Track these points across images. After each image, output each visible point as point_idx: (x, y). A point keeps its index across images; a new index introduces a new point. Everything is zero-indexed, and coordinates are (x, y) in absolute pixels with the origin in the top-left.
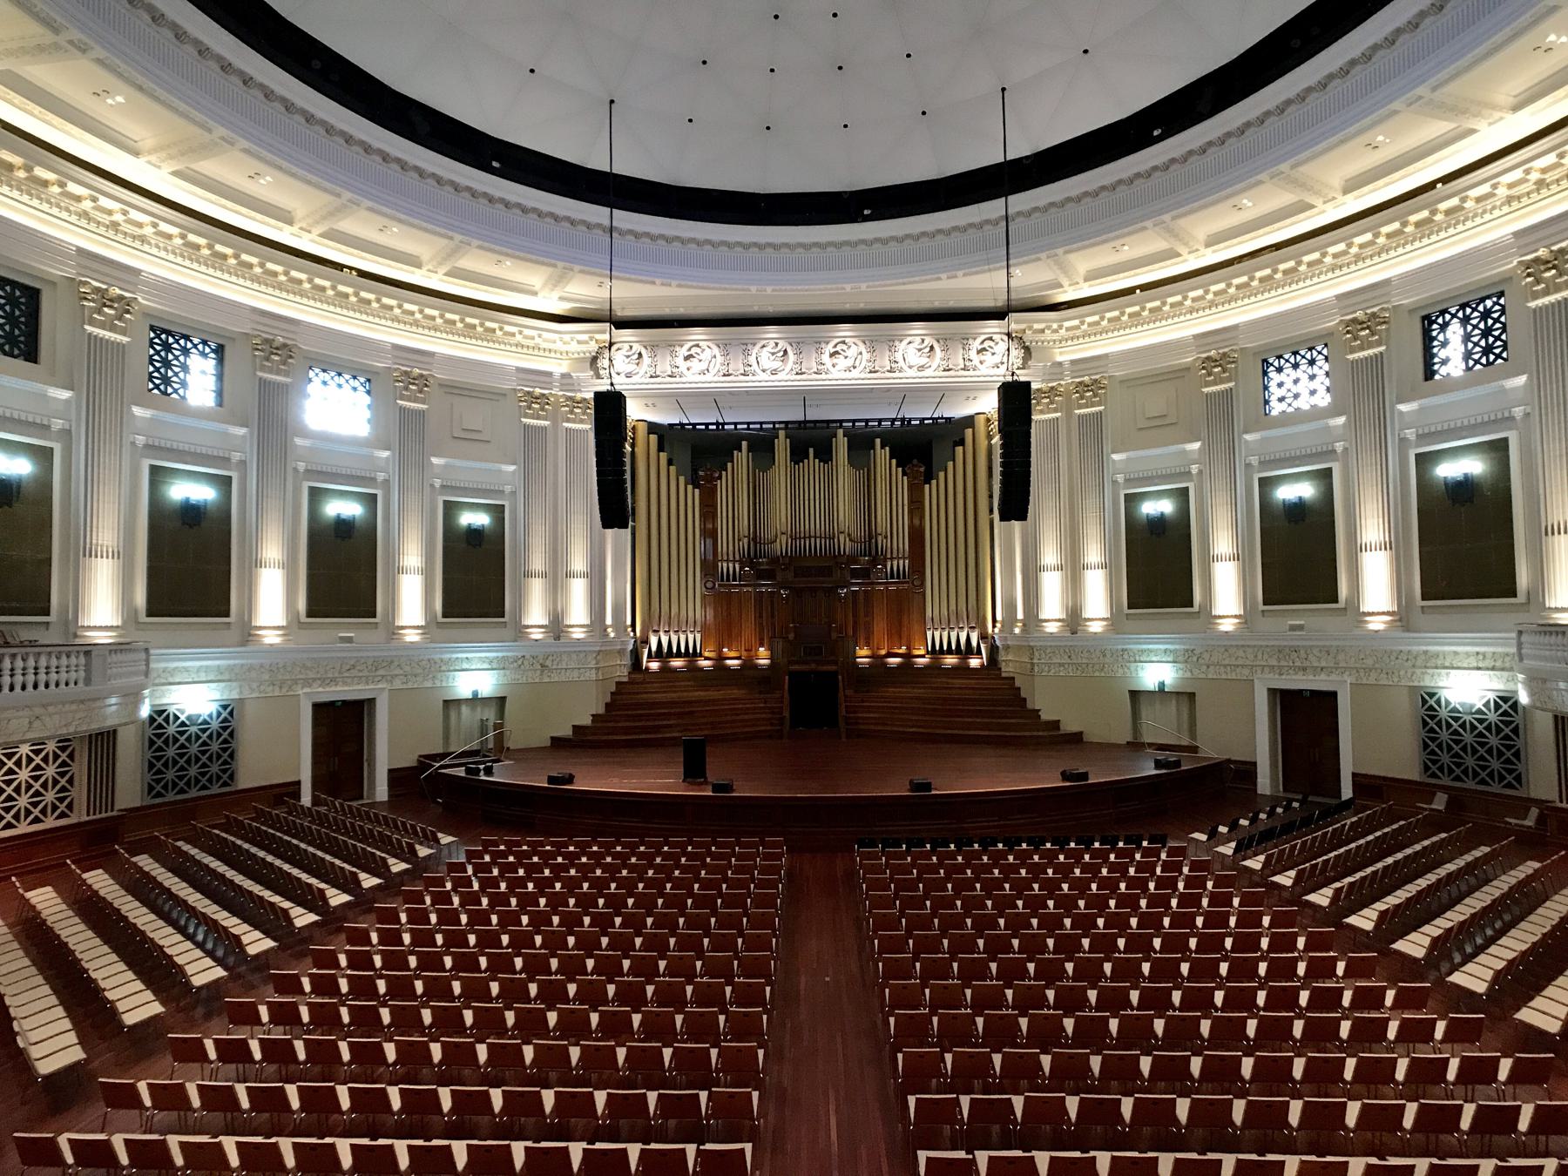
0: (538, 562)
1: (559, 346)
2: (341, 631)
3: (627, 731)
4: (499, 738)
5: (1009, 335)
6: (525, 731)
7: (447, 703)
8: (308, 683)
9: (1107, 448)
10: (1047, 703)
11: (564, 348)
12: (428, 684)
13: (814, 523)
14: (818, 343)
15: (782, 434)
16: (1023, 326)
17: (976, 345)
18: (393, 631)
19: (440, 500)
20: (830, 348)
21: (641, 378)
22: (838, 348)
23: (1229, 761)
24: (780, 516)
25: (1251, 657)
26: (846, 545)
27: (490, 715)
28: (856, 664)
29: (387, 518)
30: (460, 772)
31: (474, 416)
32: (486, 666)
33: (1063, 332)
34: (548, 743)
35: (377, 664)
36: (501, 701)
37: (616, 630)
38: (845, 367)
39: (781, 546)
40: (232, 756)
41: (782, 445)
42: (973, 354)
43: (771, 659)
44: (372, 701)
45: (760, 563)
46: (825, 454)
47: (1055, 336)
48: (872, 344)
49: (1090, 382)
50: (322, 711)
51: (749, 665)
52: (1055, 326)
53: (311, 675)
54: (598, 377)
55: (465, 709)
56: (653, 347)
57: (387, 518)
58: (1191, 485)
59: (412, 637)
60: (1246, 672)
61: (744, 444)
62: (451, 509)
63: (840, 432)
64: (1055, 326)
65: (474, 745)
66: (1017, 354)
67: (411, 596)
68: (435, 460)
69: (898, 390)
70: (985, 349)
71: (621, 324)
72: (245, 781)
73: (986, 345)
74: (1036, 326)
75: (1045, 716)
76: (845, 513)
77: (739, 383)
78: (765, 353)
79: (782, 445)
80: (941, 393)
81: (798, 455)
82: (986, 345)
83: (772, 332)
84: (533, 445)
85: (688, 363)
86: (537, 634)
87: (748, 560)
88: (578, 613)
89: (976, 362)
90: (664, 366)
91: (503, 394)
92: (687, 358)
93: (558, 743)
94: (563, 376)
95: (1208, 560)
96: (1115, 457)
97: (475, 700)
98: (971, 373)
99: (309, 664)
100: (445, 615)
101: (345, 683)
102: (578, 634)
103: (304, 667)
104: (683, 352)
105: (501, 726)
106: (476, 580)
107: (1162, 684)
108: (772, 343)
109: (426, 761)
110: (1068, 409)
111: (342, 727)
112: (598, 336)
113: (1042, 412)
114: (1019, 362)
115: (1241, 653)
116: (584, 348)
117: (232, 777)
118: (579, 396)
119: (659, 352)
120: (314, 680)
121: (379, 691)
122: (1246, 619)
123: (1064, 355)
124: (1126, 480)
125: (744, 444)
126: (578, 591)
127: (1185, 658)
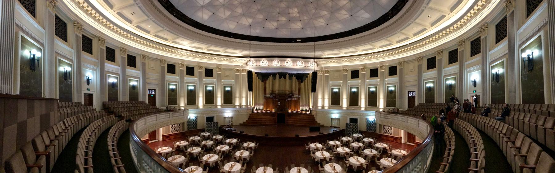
0: (238, 95)
1: (241, 61)
2: (210, 106)
6: (236, 123)
13: (282, 88)
14: (284, 61)
18: (216, 106)
26: (287, 92)
27: (230, 119)
30: (227, 129)
31: (227, 73)
38: (289, 64)
39: (277, 92)
41: (277, 75)
46: (285, 78)
48: (293, 61)
49: (327, 70)
51: (271, 112)
56: (256, 61)
59: (219, 107)
66: (316, 65)
67: (219, 101)
71: (251, 57)
72: (198, 128)
75: (318, 122)
76: (288, 88)
77: (271, 67)
79: (277, 75)
80: (304, 70)
81: (280, 78)
83: (276, 59)
84: (237, 77)
86: (237, 107)
87: (271, 94)
88: (244, 103)
90: (258, 64)
91: (232, 69)
93: (241, 124)
95: (342, 99)
97: (228, 117)
102: (244, 107)
104: (261, 62)
106: (228, 99)
110: (324, 74)
123: (323, 66)
126: (244, 100)
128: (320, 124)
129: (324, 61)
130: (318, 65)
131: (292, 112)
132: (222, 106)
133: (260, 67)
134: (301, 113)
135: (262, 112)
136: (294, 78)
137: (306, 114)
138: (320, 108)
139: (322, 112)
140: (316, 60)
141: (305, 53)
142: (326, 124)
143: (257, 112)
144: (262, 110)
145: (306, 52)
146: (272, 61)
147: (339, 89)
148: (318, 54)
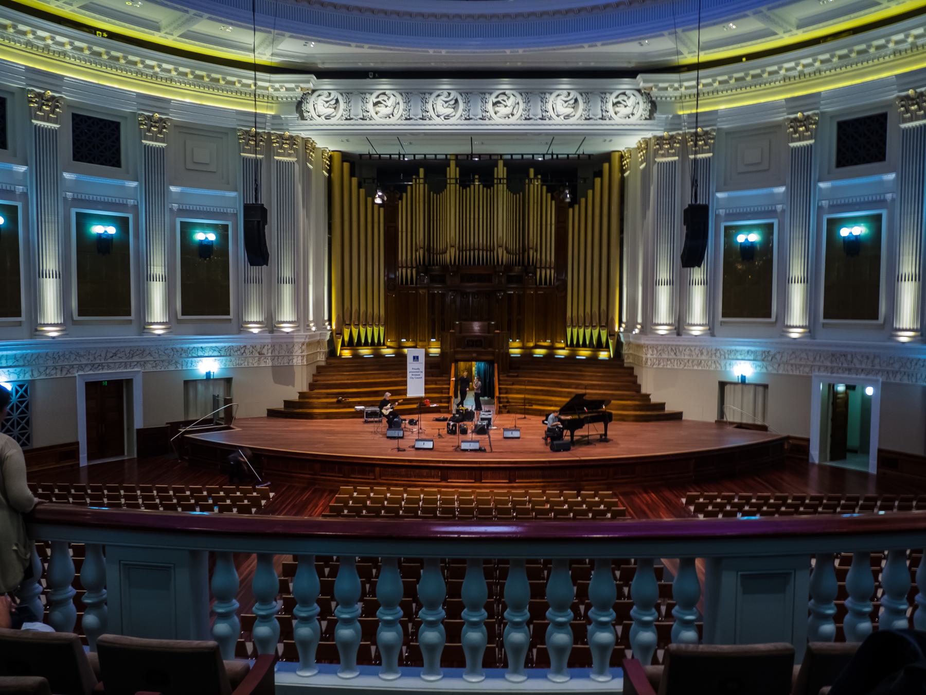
3: (328, 405)
4: (229, 412)
5: (639, 91)
7: (186, 382)
8: (81, 367)
9: (713, 188)
10: (652, 386)
11: (276, 94)
12: (172, 368)
13: (479, 239)
15: (453, 164)
16: (650, 85)
17: (612, 99)
18: (143, 325)
19: (178, 221)
20: (492, 99)
21: (338, 118)
22: (499, 99)
23: (788, 438)
24: (450, 232)
25: (811, 358)
26: (502, 255)
27: (220, 392)
28: (508, 354)
29: (137, 236)
32: (216, 353)
33: (683, 89)
34: (265, 415)
35: (133, 352)
36: (228, 381)
37: (316, 325)
38: (505, 112)
39: (450, 255)
40: (27, 423)
41: (453, 171)
43: (441, 348)
44: (129, 382)
45: (431, 268)
46: (488, 181)
48: (527, 95)
50: (93, 388)
52: (676, 85)
53: (84, 362)
54: (303, 118)
55: (200, 387)
56: (348, 94)
57: (137, 236)
58: (775, 222)
59: (159, 330)
60: (807, 370)
61: (422, 170)
62: (186, 229)
63: (501, 163)
64: (676, 85)
65: (209, 415)
66: (642, 109)
68: (173, 189)
69: (547, 134)
70: (619, 102)
71: (322, 74)
73: (620, 99)
74: (661, 85)
76: (503, 230)
78: (440, 102)
79: (453, 171)
80: (583, 136)
81: (464, 182)
82: (620, 99)
83: (445, 85)
85: (378, 109)
87: (425, 267)
90: (357, 111)
92: (375, 104)
93: (273, 414)
94: (273, 117)
95: (786, 281)
96: (719, 195)
98: (607, 122)
99: (82, 353)
100: (183, 314)
101: (109, 367)
103: (78, 355)
104: (373, 99)
105: (230, 401)
107: (743, 378)
108: (445, 93)
109: (175, 426)
110: (683, 152)
111: (108, 398)
112: (302, 85)
113: (663, 156)
114: (647, 114)
115: (804, 355)
116: (291, 94)
117: (28, 439)
118: (287, 134)
119: (353, 99)
120: (86, 365)
121: (135, 372)
122: (811, 329)
124: (726, 215)
125: (422, 170)
127: (764, 357)
128: (661, 406)
129: (688, 81)
130: (654, 107)
131: (527, 356)
132: (171, 322)
133: (367, 126)
134: (571, 360)
135: (378, 356)
136: (535, 186)
137: (593, 361)
138: (662, 330)
139: (675, 349)
140: (641, 81)
141: (586, 49)
142: (697, 408)
143: (356, 356)
144: (376, 345)
145: (592, 40)
146: (424, 95)
147: (768, 229)
148: (657, 46)
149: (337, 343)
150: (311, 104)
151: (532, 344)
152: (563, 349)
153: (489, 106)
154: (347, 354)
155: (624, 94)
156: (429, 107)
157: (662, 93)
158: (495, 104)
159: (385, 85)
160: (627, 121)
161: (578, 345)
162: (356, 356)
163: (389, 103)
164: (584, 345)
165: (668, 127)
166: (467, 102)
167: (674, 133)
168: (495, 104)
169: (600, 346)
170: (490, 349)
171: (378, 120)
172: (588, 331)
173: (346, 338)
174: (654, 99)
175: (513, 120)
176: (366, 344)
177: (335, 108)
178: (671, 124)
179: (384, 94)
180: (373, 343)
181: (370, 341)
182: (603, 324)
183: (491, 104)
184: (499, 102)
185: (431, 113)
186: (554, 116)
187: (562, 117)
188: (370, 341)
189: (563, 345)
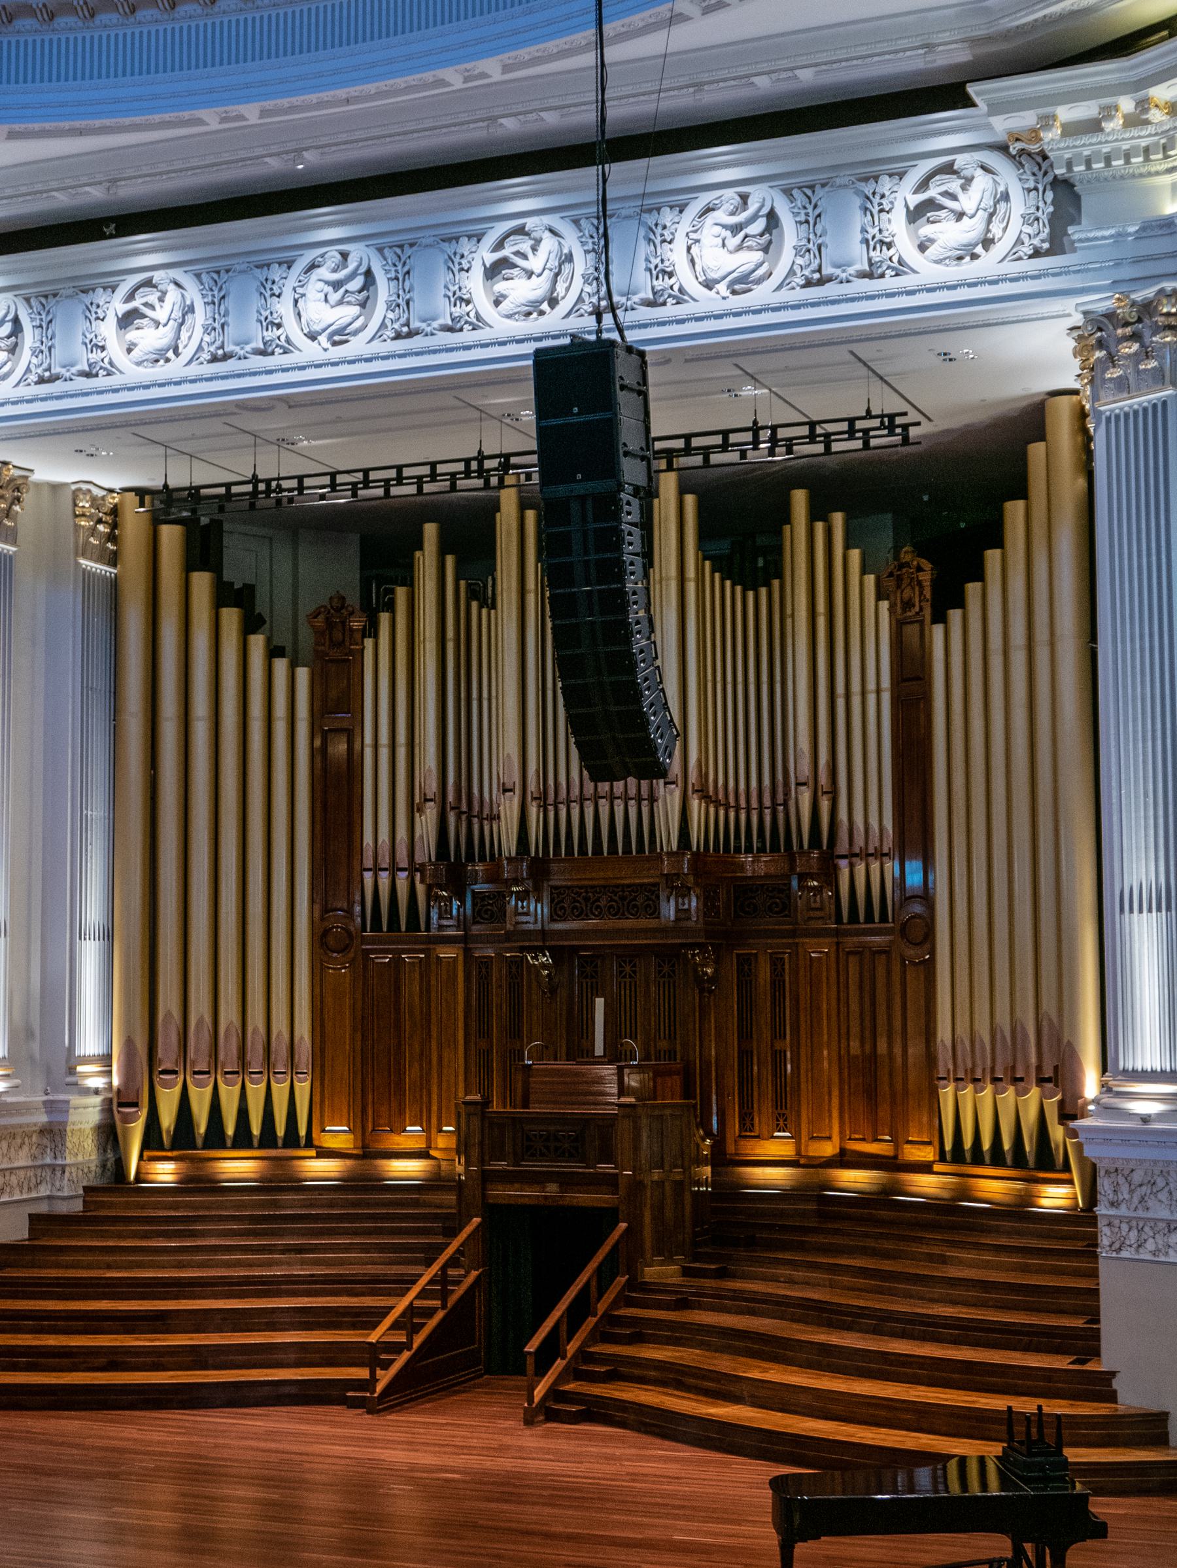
5: (1003, 148)
14: (450, 239)
42: (896, 224)
47: (1143, 137)
64: (1127, 104)
66: (1022, 214)
74: (1066, 113)
83: (328, 226)
89: (905, 246)
113: (1122, 385)
114: (1041, 236)
119: (59, 311)
128: (1152, 1427)
130: (1065, 198)
133: (94, 396)
135: (282, 1182)
143: (198, 1183)
149: (127, 1133)
150: (680, 243)
151: (828, 1149)
152: (925, 1168)
153: (896, 224)
154: (165, 1172)
155: (948, 169)
156: (676, 255)
157: (1086, 145)
158: (916, 215)
159: (146, 253)
160: (968, 269)
161: (977, 1157)
162: (198, 1183)
163: (968, 202)
164: (997, 1158)
165: (1127, 272)
166: (810, 221)
167: (1149, 292)
168: (916, 215)
169: (1045, 1162)
170: (605, 1167)
171: (130, 371)
172: (255, 1093)
173: (167, 1119)
174: (1060, 171)
175: (988, 263)
176: (243, 1139)
177: (766, 249)
178: (1137, 261)
179: (521, 231)
180: (268, 1138)
181: (256, 1130)
182: (1048, 1073)
183: (477, 273)
184: (930, 205)
185: (292, 329)
186: (694, 287)
187: (722, 287)
188: (256, 1130)
189: (927, 1154)
